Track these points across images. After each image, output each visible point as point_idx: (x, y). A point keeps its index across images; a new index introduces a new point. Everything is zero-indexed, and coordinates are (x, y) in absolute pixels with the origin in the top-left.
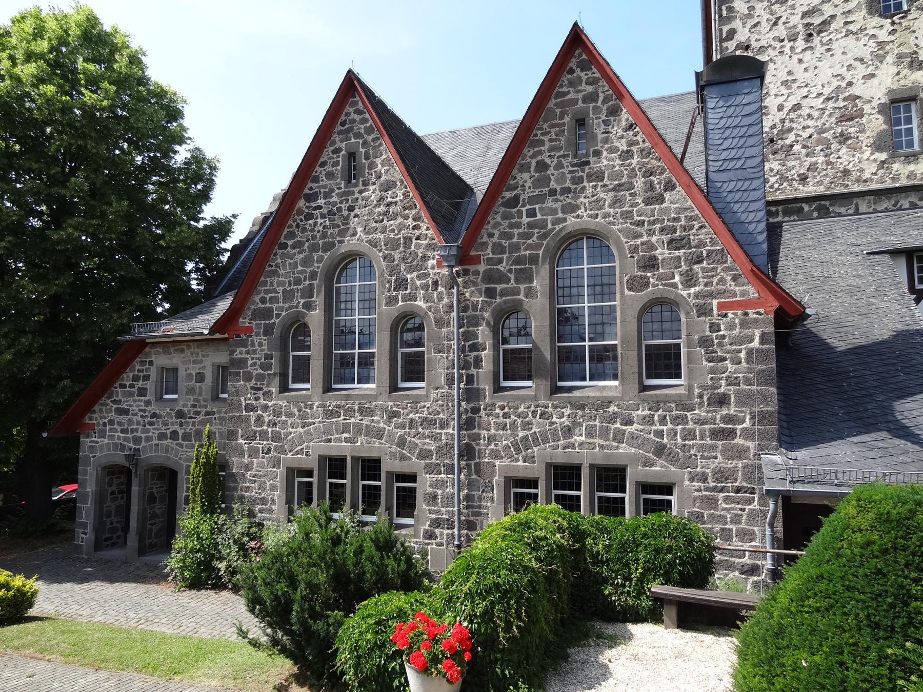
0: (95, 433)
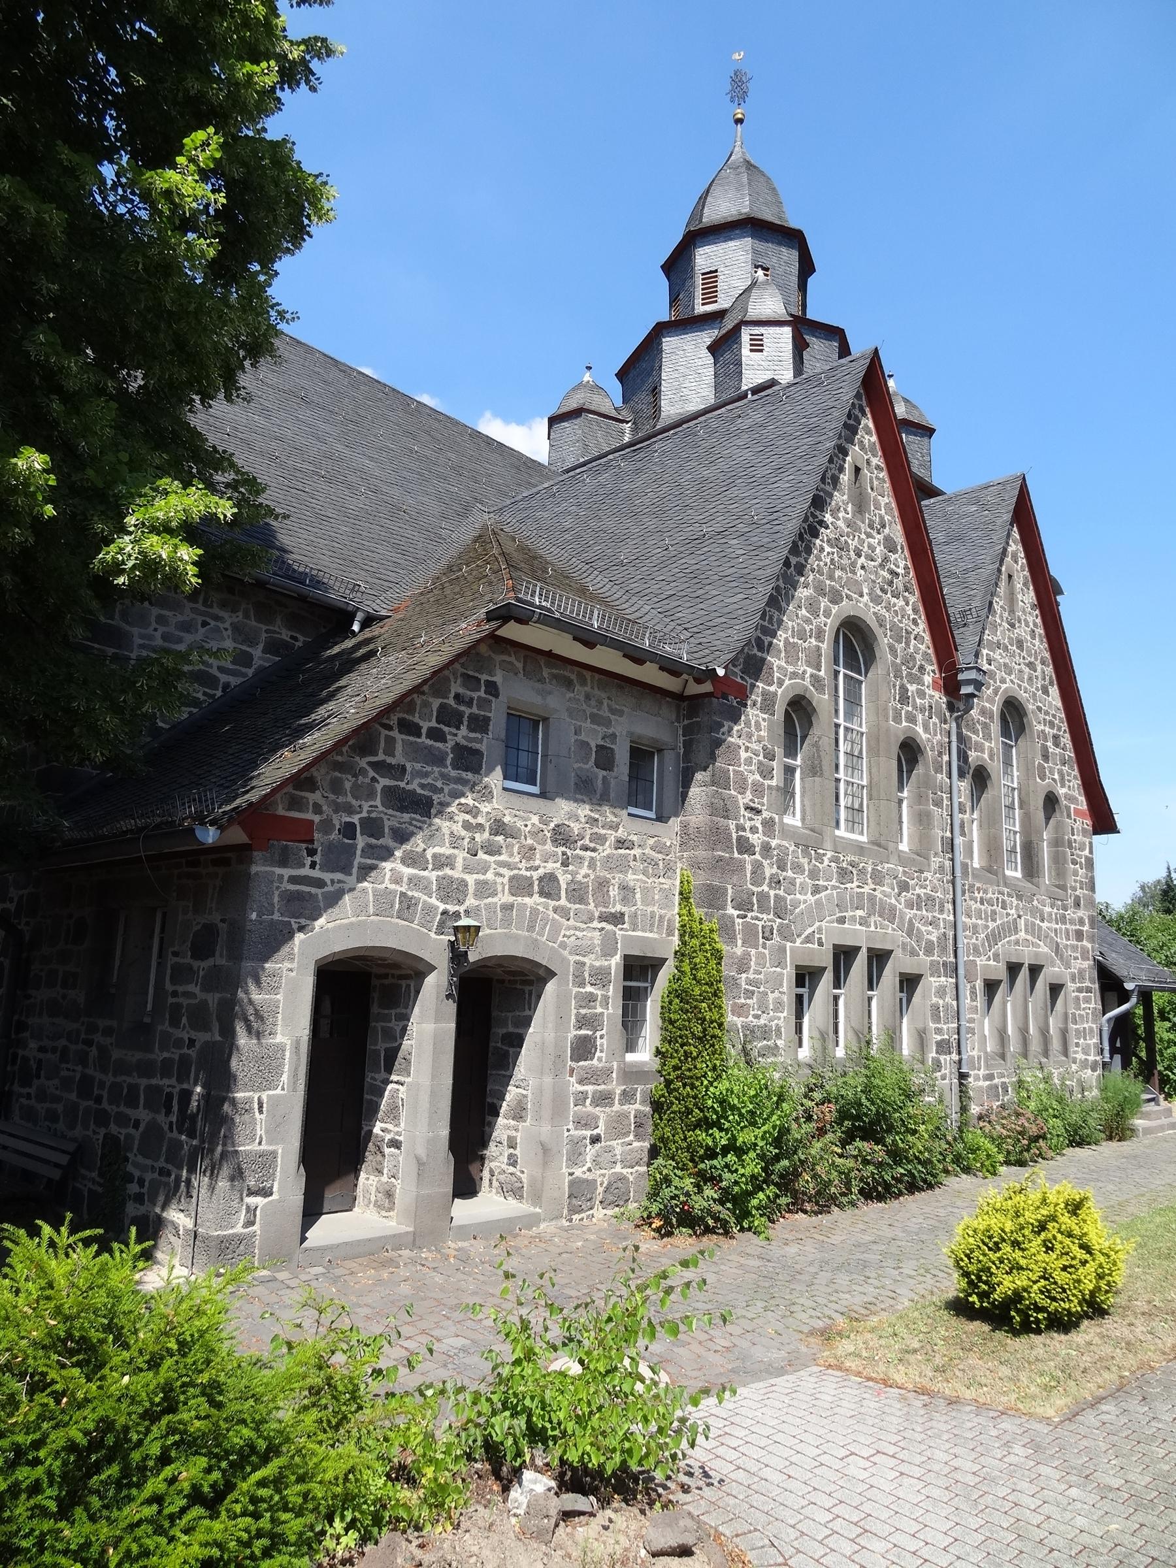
0: (312, 852)
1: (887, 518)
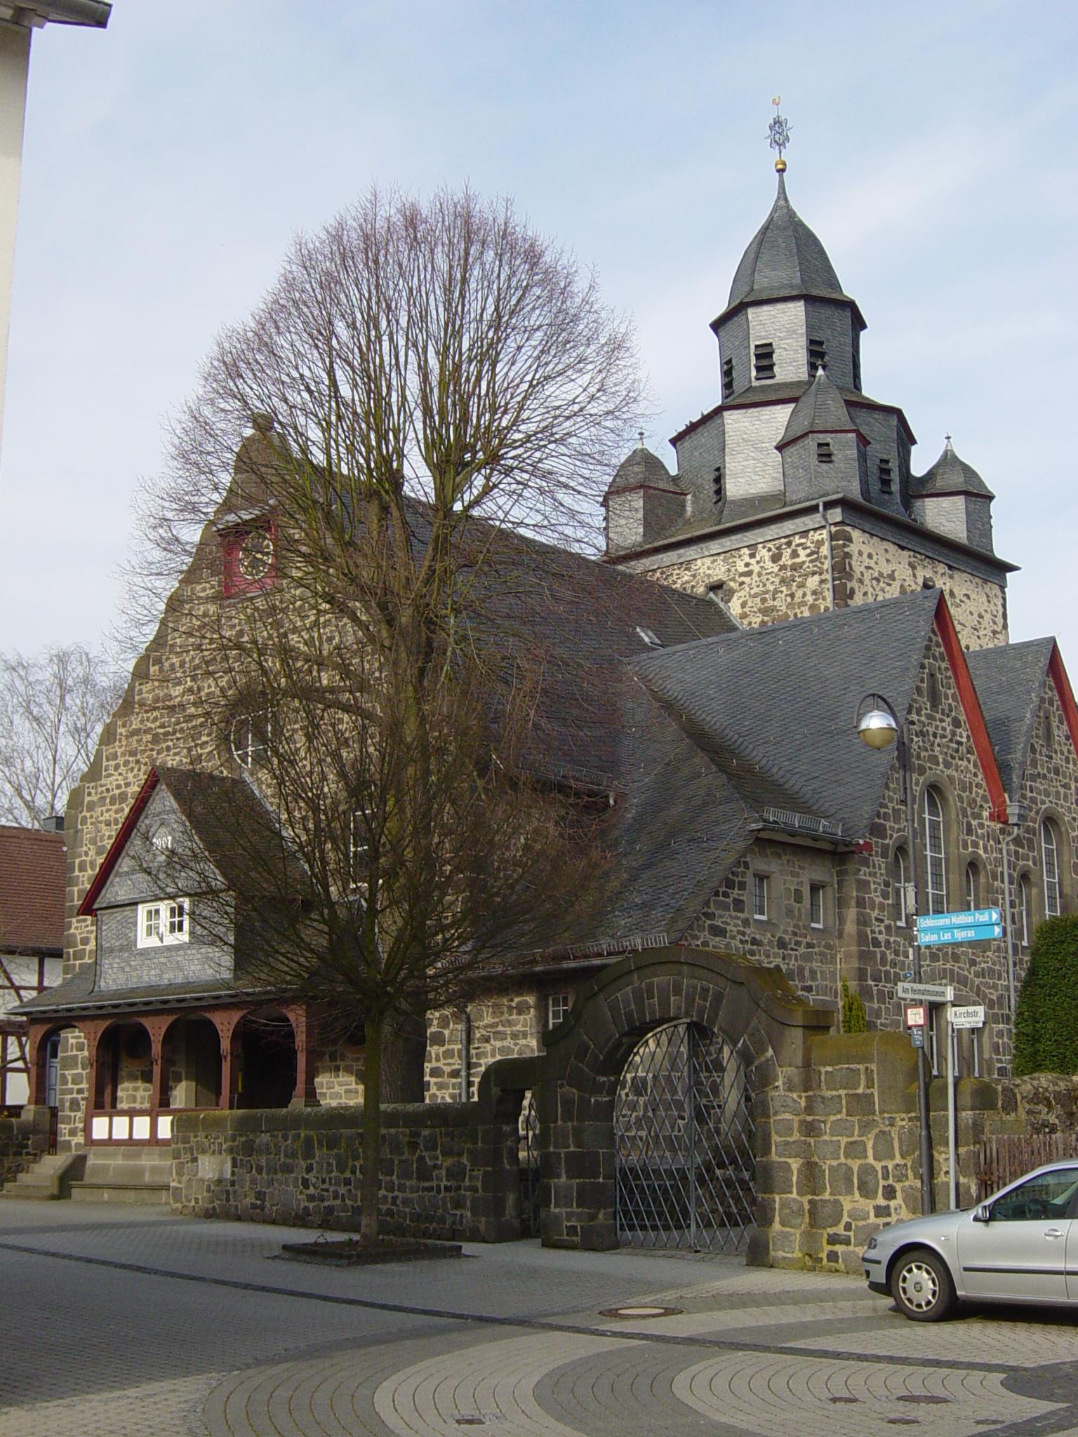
1: (953, 704)
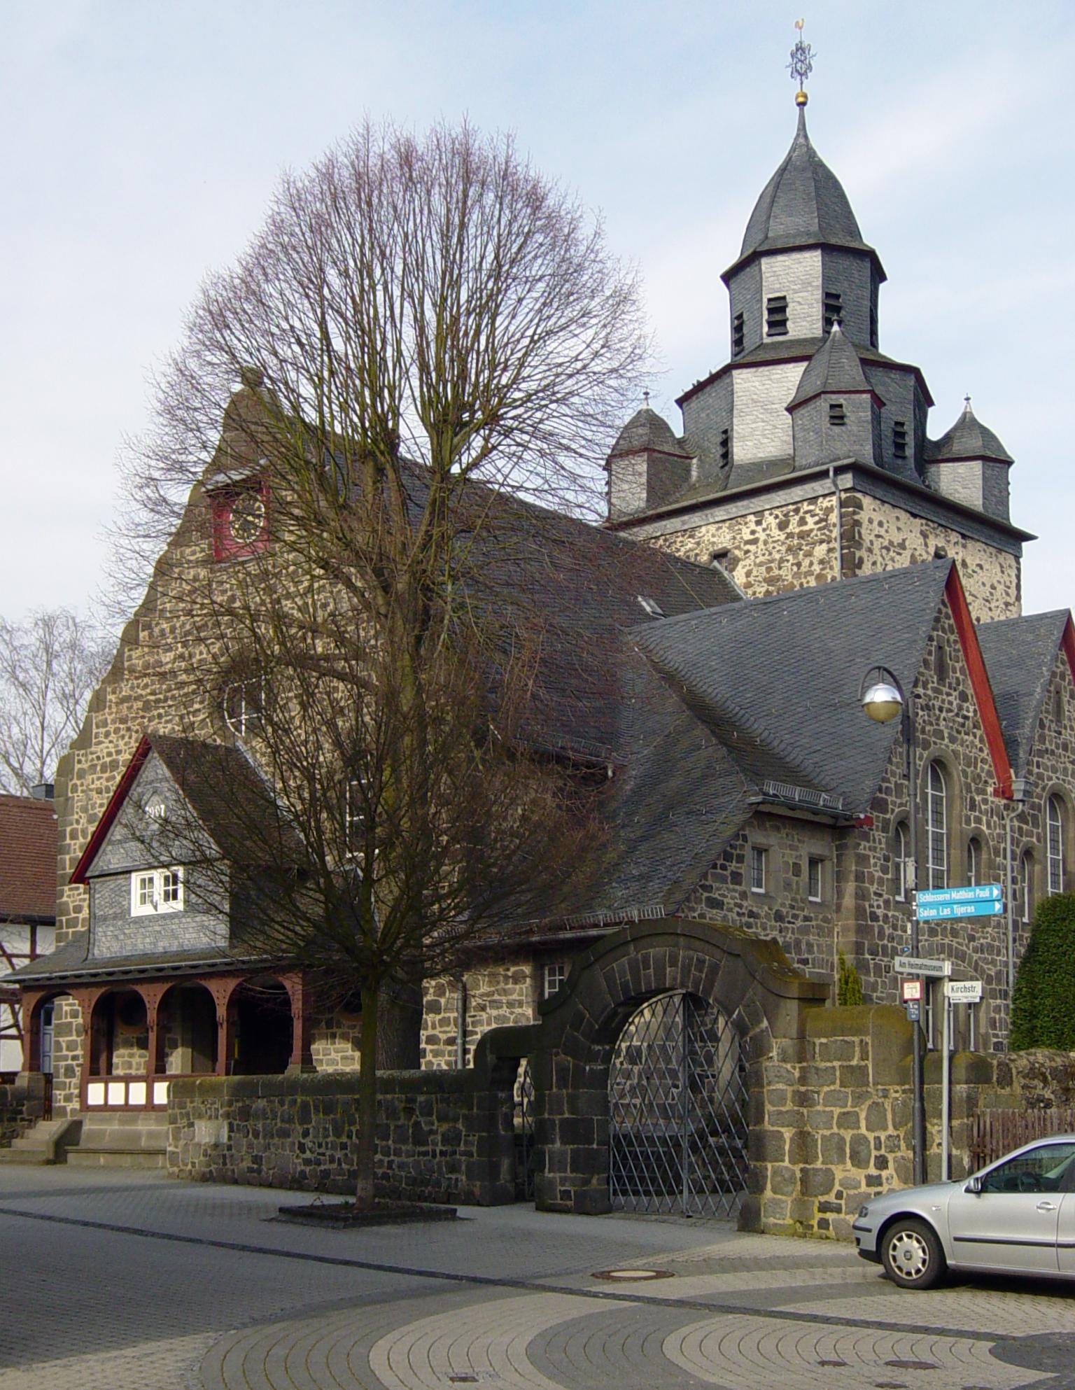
1: (961, 677)
